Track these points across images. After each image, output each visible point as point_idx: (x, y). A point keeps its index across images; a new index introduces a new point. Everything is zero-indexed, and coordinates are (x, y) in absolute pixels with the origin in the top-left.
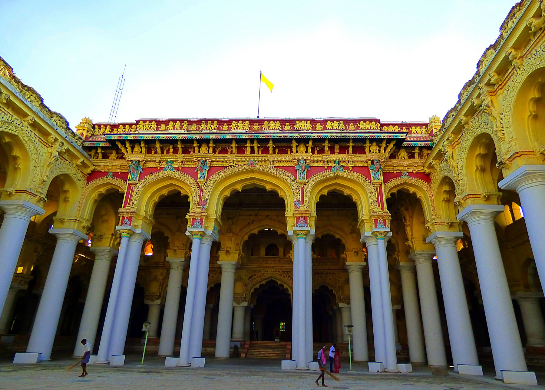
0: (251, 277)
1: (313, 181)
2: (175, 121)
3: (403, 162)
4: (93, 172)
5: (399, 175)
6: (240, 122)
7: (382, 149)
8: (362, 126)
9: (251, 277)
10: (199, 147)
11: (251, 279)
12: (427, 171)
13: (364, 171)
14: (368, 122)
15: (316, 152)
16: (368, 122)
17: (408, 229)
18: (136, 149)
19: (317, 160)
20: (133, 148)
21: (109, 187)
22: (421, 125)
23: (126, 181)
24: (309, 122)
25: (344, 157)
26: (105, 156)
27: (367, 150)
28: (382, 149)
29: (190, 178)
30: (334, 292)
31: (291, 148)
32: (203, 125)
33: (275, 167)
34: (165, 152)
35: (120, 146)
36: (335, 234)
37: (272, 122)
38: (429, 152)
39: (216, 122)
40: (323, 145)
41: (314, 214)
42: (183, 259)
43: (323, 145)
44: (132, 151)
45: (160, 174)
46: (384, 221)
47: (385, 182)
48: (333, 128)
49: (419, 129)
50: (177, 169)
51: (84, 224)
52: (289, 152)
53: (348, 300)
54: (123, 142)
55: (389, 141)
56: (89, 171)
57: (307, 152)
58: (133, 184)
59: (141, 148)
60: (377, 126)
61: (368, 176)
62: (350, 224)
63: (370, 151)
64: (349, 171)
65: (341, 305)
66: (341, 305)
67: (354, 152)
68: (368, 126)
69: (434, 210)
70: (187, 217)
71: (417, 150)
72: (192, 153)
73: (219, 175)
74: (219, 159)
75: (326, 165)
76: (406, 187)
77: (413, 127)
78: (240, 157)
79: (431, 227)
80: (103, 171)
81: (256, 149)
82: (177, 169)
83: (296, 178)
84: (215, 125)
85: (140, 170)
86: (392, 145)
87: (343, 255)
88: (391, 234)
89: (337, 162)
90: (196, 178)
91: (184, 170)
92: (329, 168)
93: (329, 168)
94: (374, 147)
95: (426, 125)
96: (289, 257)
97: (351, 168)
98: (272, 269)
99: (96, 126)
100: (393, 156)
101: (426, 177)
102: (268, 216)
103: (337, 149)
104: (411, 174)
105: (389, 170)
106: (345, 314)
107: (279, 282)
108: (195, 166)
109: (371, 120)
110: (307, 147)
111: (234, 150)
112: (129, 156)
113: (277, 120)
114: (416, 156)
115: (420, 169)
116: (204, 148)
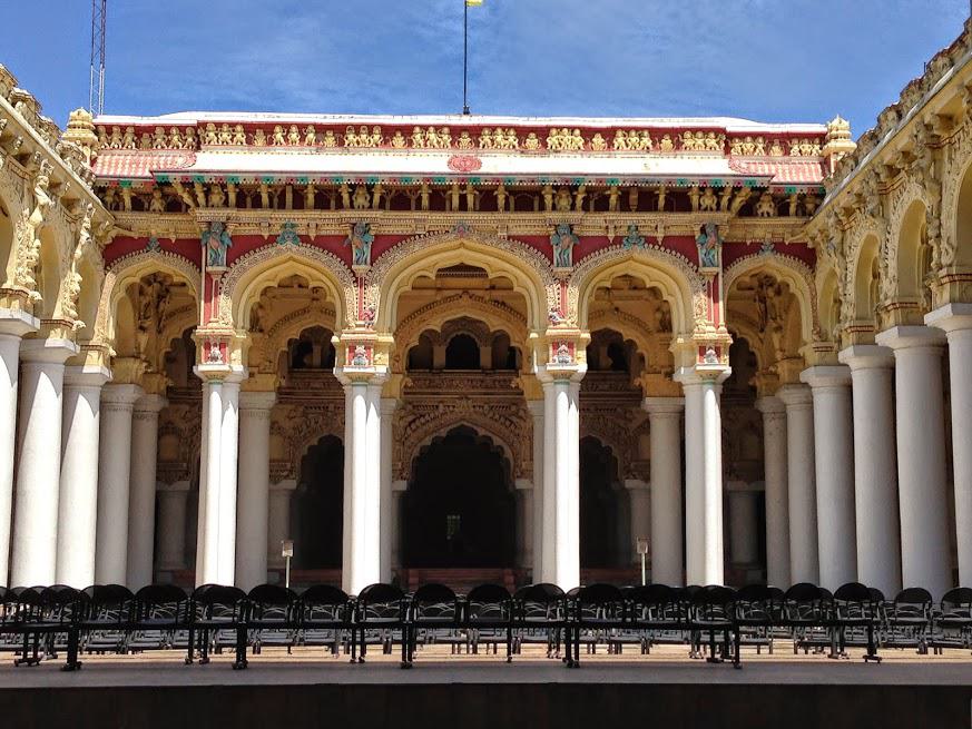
0: (414, 421)
1: (586, 269)
2: (286, 127)
3: (764, 227)
4: (117, 239)
5: (756, 248)
6: (432, 129)
7: (725, 201)
8: (688, 143)
9: (414, 421)
10: (351, 194)
11: (413, 426)
12: (810, 246)
13: (683, 247)
14: (700, 134)
15: (592, 204)
16: (700, 134)
17: (776, 338)
18: (216, 198)
19: (594, 224)
20: (207, 193)
21: (150, 270)
22: (811, 137)
23: (196, 261)
24: (577, 132)
25: (647, 219)
26: (139, 204)
27: (695, 200)
28: (725, 201)
29: (336, 261)
30: (615, 452)
31: (542, 198)
32: (351, 137)
33: (509, 238)
34: (276, 200)
35: (180, 190)
36: (622, 331)
37: (499, 131)
38: (818, 201)
39: (377, 131)
40: (608, 192)
41: (587, 336)
42: (273, 397)
43: (608, 192)
44: (207, 201)
45: (272, 250)
46: (718, 351)
47: (724, 267)
48: (627, 145)
49: (806, 147)
50: (305, 239)
51: (113, 352)
52: (536, 204)
53: (644, 471)
54: (188, 184)
55: (737, 189)
56: (109, 241)
57: (573, 207)
58: (216, 273)
59: (227, 195)
60: (718, 143)
61: (692, 258)
62: (658, 310)
63: (700, 205)
64: (656, 247)
65: (629, 484)
66: (629, 484)
67: (669, 208)
68: (700, 142)
69: (815, 323)
70: (335, 339)
71: (794, 198)
72: (333, 203)
73: (398, 258)
74: (394, 222)
75: (611, 235)
76: (769, 271)
77: (796, 141)
78: (437, 218)
79: (807, 354)
80: (135, 235)
81: (470, 199)
82: (305, 239)
83: (552, 262)
84: (377, 137)
85: (227, 241)
86: (743, 193)
87: (637, 382)
88: (728, 371)
89: (633, 228)
90: (349, 263)
91: (322, 243)
92: (618, 241)
93: (618, 241)
94: (708, 201)
95: (822, 138)
96: (517, 387)
97: (660, 240)
98: (464, 402)
99: (102, 129)
100: (748, 210)
101: (806, 256)
102: (466, 291)
103: (634, 197)
104: (780, 248)
105: (739, 235)
106: (637, 504)
107: (482, 432)
108: (342, 233)
109: (706, 131)
110: (574, 198)
111: (425, 202)
112: (204, 214)
113: (510, 127)
114: (792, 209)
115: (798, 238)
116: (360, 201)
